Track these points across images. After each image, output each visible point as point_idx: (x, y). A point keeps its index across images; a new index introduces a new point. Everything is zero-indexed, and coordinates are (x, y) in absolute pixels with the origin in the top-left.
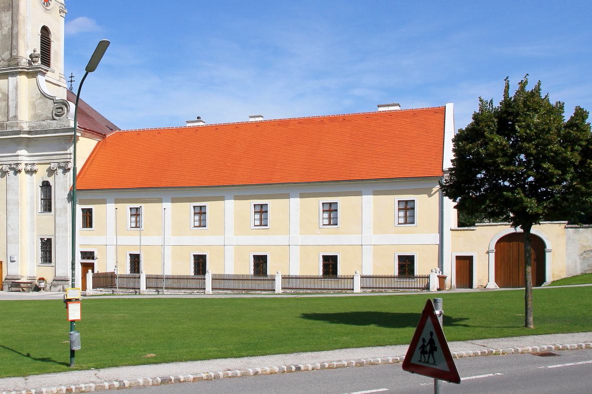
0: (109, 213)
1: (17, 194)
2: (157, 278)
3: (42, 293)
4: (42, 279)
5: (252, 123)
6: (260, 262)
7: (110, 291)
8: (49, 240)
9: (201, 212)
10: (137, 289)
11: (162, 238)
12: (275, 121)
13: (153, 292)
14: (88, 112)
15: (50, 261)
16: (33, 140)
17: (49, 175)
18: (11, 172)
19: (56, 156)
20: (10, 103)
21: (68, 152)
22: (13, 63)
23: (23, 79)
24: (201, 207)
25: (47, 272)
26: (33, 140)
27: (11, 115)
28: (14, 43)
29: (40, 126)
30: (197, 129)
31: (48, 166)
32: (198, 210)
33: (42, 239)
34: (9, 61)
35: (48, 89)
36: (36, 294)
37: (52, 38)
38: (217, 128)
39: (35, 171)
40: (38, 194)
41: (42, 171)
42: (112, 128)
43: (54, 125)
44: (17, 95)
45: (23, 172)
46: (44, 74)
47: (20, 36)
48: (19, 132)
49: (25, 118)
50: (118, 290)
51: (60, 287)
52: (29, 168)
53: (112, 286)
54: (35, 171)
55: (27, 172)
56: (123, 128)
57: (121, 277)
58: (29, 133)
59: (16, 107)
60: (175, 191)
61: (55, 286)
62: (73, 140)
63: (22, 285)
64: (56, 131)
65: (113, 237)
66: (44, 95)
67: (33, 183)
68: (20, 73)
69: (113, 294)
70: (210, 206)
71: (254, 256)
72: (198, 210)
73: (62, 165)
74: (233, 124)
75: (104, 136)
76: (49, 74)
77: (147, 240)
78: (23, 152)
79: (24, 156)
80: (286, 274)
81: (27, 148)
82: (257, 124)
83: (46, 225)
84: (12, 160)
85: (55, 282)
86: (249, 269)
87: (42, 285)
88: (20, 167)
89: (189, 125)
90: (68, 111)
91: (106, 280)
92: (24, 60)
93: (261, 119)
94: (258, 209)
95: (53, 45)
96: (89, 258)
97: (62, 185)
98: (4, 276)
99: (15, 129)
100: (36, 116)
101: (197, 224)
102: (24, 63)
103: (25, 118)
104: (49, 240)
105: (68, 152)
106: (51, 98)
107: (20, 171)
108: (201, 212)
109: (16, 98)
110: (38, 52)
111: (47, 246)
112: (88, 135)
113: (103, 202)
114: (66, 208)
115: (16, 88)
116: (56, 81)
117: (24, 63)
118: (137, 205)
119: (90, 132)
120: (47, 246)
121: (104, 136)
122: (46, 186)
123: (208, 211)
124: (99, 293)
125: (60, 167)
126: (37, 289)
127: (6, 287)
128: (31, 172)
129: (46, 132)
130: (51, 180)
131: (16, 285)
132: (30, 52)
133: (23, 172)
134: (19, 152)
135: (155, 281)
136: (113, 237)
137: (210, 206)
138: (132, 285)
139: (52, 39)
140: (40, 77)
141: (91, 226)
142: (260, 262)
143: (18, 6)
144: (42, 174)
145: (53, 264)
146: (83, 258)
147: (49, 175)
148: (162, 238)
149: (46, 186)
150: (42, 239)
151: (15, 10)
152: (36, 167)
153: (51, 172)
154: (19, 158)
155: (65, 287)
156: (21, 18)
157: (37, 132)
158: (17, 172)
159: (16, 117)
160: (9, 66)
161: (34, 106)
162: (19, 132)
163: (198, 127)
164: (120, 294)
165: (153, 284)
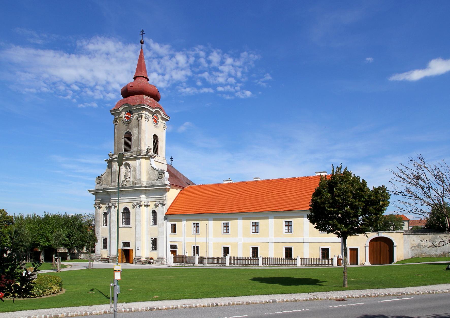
0: (185, 226)
1: (140, 216)
2: (204, 258)
3: (152, 265)
4: (152, 258)
5: (254, 182)
6: (289, 252)
7: (181, 265)
8: (155, 239)
9: (227, 226)
10: (194, 263)
11: (210, 239)
12: (265, 180)
13: (201, 265)
14: (178, 176)
15: (156, 250)
16: (148, 190)
17: (156, 208)
18: (138, 206)
19: (158, 198)
20: (137, 172)
21: (164, 196)
22: (139, 153)
23: (143, 160)
24: (256, 222)
25: (154, 255)
26: (148, 190)
27: (138, 178)
28: (139, 143)
29: (151, 183)
30: (227, 184)
31: (155, 203)
32: (254, 224)
33: (152, 239)
34: (137, 152)
35: (155, 165)
36: (149, 265)
37: (159, 140)
38: (237, 184)
39: (149, 206)
40: (151, 216)
41: (152, 205)
42: (189, 183)
43: (158, 183)
44: (140, 168)
45: (143, 206)
46: (154, 158)
47: (142, 140)
48: (141, 187)
49: (144, 179)
50: (185, 264)
51: (160, 262)
52: (146, 204)
53: (182, 262)
54: (149, 206)
55: (145, 206)
56: (198, 183)
57: (190, 258)
58: (146, 187)
59: (140, 174)
60: (215, 215)
61: (158, 262)
62: (166, 190)
63: (142, 261)
64: (158, 186)
65: (186, 237)
66: (153, 169)
67: (148, 211)
68: (142, 158)
69: (183, 266)
70: (231, 223)
71: (285, 248)
72: (225, 225)
73: (161, 202)
74: (245, 182)
75: (183, 188)
76: (156, 157)
77: (192, 239)
78: (143, 196)
79: (143, 198)
80: (302, 257)
81: (145, 194)
82: (256, 182)
83: (154, 232)
84: (138, 200)
85: (158, 260)
86: (283, 255)
87: (152, 261)
88: (141, 204)
89: (225, 182)
90: (164, 176)
91: (179, 259)
92: (144, 152)
93: (259, 179)
94: (287, 224)
95: (159, 143)
96: (174, 248)
97: (162, 212)
98: (134, 257)
99: (140, 185)
100: (149, 179)
101: (225, 231)
102: (144, 153)
103: (144, 179)
104: (155, 239)
105: (164, 196)
106: (157, 170)
107: (141, 205)
108: (227, 226)
109: (140, 170)
110: (151, 147)
111: (154, 242)
112: (175, 187)
113: (181, 220)
114: (163, 224)
115: (140, 165)
116: (160, 162)
117: (144, 153)
118: (197, 222)
119: (174, 186)
120: (154, 242)
121: (183, 188)
122: (154, 213)
123: (259, 225)
124: (177, 265)
125: (160, 204)
126: (149, 263)
127: (134, 262)
128: (147, 206)
129: (154, 186)
130: (156, 210)
131: (139, 261)
132: (147, 147)
133: (143, 206)
134: (141, 196)
135: (203, 260)
136: (186, 237)
137: (231, 223)
138: (191, 261)
139: (159, 141)
140: (151, 159)
141: (175, 232)
142: (289, 252)
143: (141, 125)
144: (152, 207)
145: (157, 251)
146: (171, 248)
147: (156, 208)
148: (210, 239)
149: (154, 213)
150: (152, 239)
151: (140, 127)
152: (149, 204)
153: (156, 206)
154: (141, 199)
155: (163, 262)
156: (142, 131)
157: (149, 187)
158: (140, 206)
159: (140, 179)
160: (137, 154)
161: (148, 174)
162: (141, 187)
163: (228, 184)
164: (186, 266)
165: (201, 261)
